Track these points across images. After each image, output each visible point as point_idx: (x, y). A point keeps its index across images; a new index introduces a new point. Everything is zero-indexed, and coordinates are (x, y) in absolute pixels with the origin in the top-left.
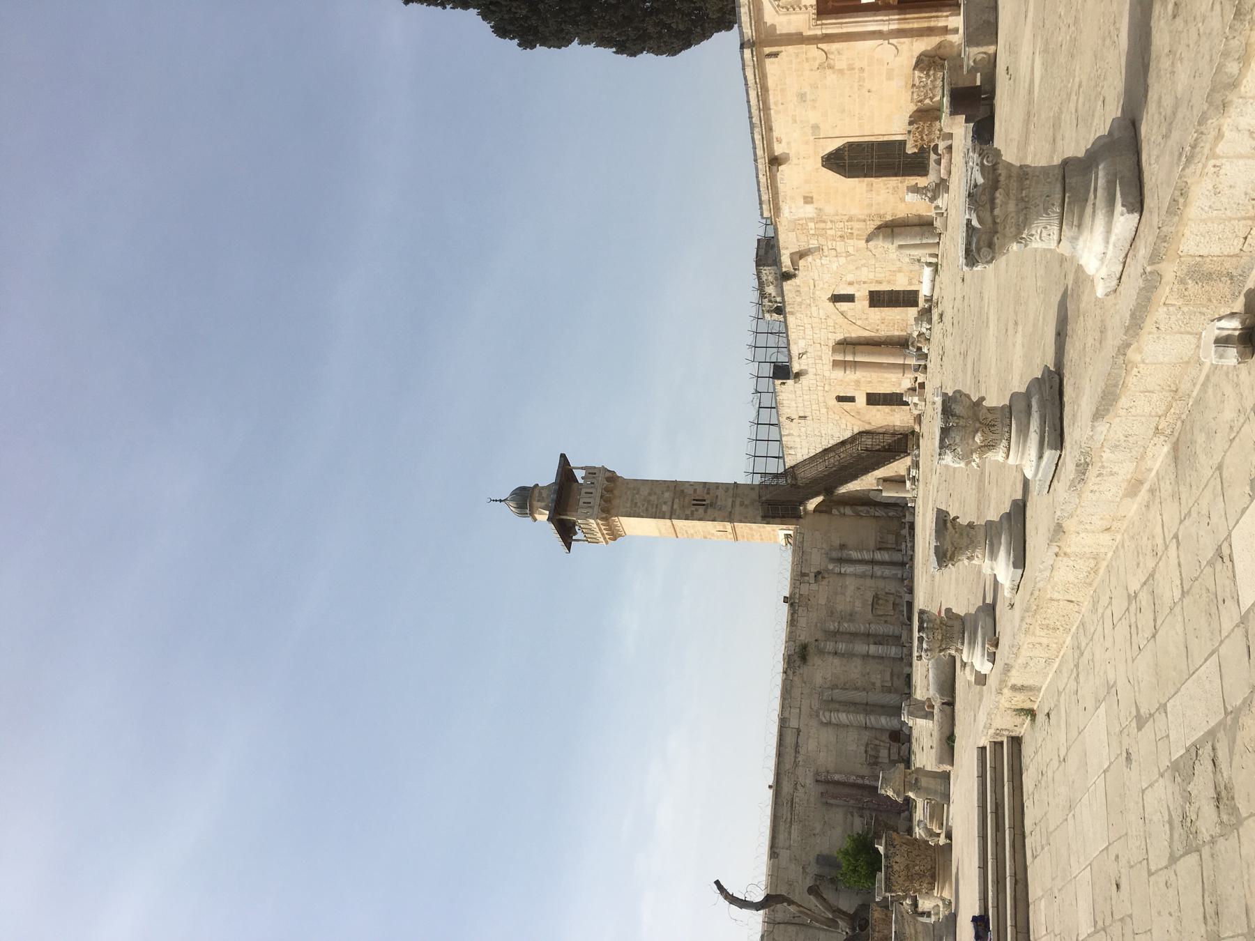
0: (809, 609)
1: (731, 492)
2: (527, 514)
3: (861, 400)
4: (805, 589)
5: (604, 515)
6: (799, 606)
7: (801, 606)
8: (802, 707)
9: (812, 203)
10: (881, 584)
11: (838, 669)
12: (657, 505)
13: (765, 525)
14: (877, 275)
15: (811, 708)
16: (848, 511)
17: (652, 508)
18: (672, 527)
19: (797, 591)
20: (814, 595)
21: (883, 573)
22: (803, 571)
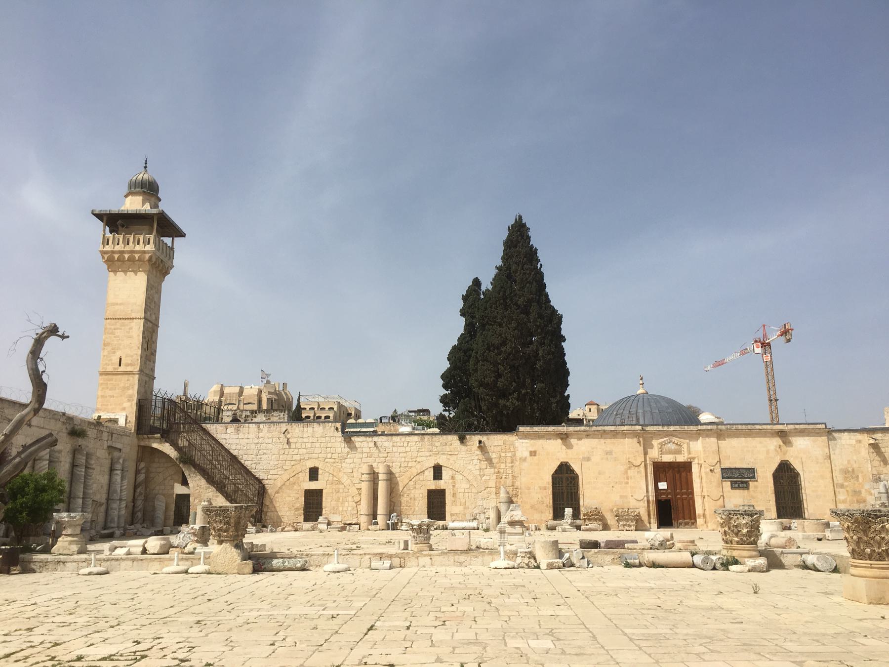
1: (151, 373)
2: (130, 189)
3: (313, 486)
4: (105, 436)
5: (154, 260)
9: (531, 456)
10: (103, 509)
12: (150, 307)
13: (135, 401)
14: (461, 495)
16: (142, 477)
21: (115, 509)
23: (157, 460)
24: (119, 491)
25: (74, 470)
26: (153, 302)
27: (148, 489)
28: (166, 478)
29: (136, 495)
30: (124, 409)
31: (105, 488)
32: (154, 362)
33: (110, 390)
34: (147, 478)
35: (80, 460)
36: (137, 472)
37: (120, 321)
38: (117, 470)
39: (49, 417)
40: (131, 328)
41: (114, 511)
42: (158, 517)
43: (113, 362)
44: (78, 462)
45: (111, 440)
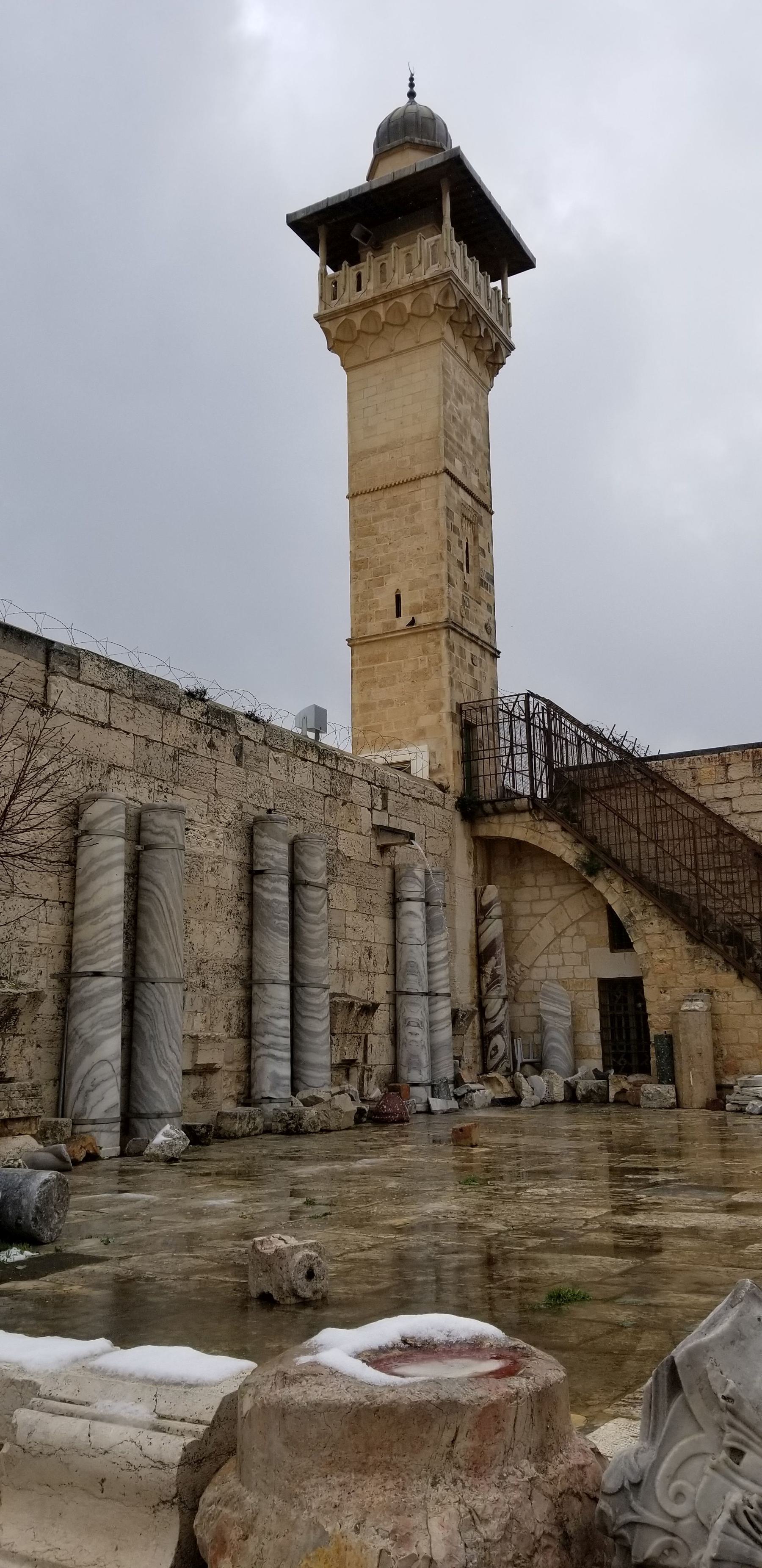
0: (328, 799)
4: (360, 791)
6: (331, 769)
7: (332, 778)
8: (115, 735)
10: (381, 1020)
11: (212, 881)
12: (461, 448)
15: (112, 767)
17: (457, 434)
18: (408, 476)
19: (357, 772)
20: (354, 821)
22: (391, 795)
23: (529, 879)
24: (423, 968)
25: (256, 889)
26: (469, 439)
27: (516, 966)
28: (564, 931)
29: (484, 985)
30: (421, 734)
31: (382, 952)
32: (491, 608)
33: (381, 687)
34: (508, 931)
35: (270, 853)
36: (482, 912)
37: (387, 495)
38: (409, 900)
39: (129, 693)
40: (416, 508)
41: (416, 1030)
42: (553, 1048)
43: (380, 609)
44: (263, 861)
45: (385, 808)
